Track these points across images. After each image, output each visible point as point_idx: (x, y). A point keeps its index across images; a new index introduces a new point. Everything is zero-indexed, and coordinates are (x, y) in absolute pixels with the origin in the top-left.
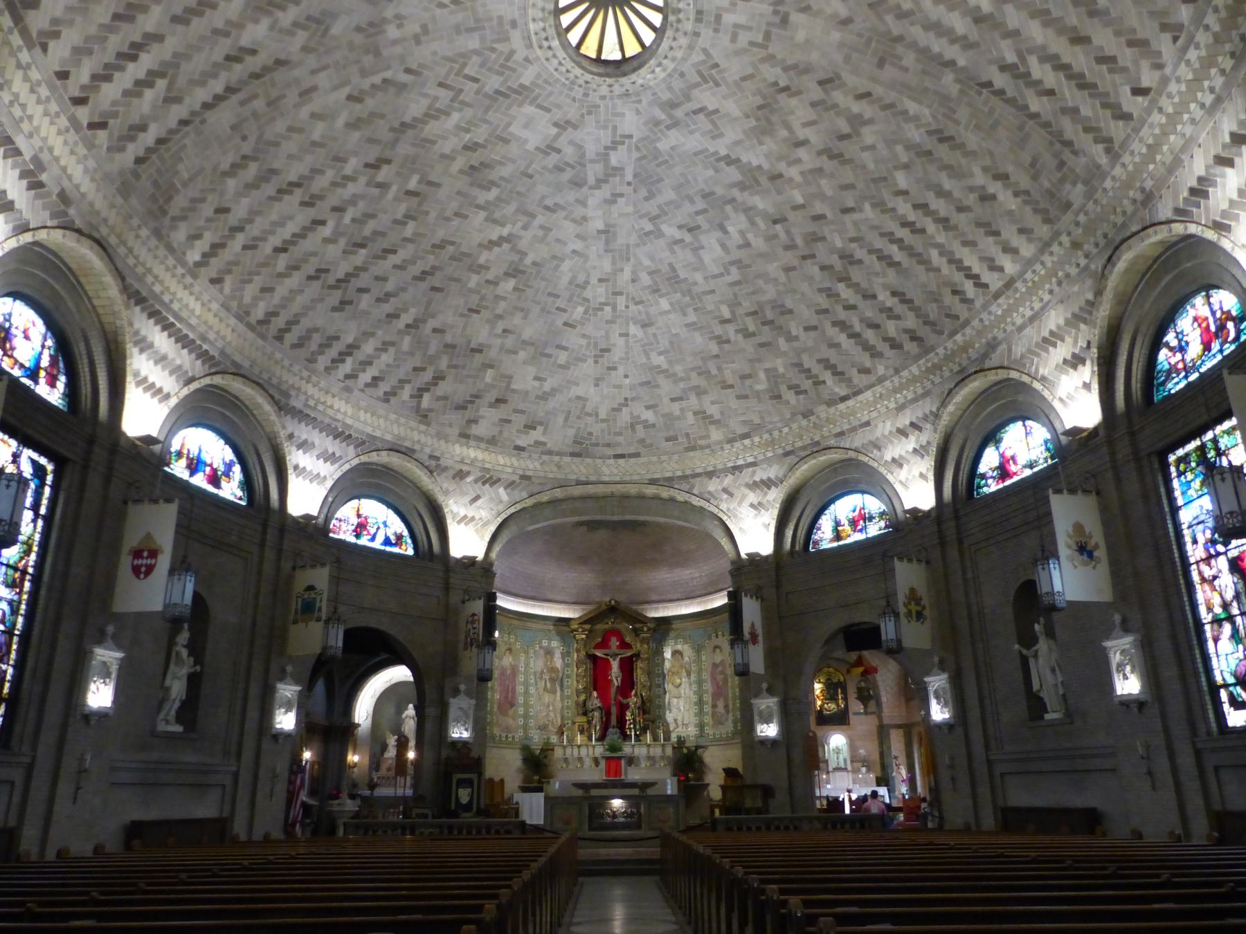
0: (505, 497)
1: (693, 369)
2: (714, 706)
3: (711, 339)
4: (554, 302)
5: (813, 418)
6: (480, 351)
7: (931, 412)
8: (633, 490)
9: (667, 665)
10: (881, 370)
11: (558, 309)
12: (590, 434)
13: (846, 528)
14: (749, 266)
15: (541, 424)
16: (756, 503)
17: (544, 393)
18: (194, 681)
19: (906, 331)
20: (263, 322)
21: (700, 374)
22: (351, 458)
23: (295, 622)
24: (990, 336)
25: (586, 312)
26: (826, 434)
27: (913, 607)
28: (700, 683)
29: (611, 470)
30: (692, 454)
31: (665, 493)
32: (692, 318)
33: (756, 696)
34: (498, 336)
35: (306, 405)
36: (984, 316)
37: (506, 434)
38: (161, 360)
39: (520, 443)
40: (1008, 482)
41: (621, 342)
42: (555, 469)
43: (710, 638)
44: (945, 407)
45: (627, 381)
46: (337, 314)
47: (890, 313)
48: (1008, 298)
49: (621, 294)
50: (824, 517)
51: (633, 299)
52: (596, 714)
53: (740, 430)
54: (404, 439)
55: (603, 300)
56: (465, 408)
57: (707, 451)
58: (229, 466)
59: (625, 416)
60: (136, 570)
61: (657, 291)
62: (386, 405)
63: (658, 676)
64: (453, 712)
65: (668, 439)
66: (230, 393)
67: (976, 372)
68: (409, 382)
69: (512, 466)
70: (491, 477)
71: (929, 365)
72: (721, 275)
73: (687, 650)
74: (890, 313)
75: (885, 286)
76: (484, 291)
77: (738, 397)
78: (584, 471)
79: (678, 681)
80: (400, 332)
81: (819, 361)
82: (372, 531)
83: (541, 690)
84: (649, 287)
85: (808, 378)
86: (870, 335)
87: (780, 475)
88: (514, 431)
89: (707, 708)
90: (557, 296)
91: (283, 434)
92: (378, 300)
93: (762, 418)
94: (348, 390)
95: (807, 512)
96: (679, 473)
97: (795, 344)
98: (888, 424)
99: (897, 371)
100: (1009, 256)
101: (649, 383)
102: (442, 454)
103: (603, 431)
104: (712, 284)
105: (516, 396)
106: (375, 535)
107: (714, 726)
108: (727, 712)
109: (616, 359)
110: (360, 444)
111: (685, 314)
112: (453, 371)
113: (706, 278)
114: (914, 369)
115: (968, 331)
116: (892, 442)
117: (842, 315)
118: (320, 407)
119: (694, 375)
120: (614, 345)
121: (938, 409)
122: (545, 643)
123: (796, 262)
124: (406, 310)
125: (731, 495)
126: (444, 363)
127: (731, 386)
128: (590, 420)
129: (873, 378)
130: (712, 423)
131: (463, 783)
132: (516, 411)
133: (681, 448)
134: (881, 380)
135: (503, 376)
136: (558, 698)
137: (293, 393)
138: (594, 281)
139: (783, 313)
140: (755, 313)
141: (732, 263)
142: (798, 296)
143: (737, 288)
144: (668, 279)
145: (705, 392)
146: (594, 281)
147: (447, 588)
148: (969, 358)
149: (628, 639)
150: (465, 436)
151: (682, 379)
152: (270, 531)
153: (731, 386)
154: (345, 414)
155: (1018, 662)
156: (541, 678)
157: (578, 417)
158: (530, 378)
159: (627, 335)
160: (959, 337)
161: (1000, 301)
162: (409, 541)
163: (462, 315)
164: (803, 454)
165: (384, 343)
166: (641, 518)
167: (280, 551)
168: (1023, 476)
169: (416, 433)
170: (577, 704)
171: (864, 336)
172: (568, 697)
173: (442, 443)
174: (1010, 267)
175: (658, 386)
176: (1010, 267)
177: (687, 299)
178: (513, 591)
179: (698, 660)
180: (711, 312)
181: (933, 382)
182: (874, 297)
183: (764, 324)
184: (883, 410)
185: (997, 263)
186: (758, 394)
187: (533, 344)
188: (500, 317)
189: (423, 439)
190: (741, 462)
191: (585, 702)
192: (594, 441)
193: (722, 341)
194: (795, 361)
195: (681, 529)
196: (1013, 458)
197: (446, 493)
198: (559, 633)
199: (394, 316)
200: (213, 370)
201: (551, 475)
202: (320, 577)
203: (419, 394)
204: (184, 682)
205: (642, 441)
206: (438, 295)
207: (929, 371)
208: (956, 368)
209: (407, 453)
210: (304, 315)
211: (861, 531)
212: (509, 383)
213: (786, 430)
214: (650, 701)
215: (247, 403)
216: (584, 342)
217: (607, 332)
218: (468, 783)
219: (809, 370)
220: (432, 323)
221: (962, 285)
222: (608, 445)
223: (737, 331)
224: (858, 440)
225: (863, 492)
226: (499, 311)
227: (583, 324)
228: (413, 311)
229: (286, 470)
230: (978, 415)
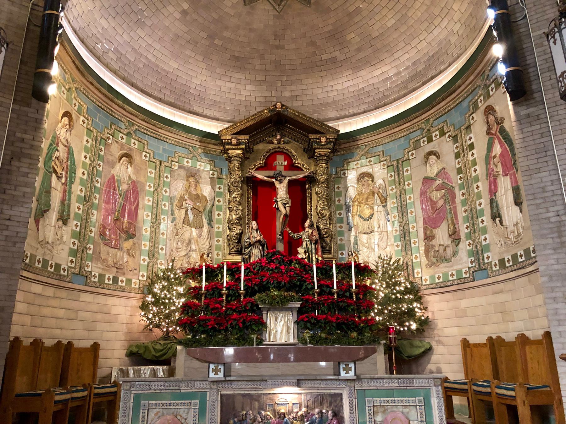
2: (428, 238)
9: (352, 192)
28: (403, 210)
43: (417, 146)
63: (340, 207)
79: (367, 212)
83: (180, 225)
107: (430, 265)
122: (187, 163)
149: (299, 162)
156: (180, 207)
172: (219, 234)
178: (139, 84)
191: (240, 235)
198: (207, 153)
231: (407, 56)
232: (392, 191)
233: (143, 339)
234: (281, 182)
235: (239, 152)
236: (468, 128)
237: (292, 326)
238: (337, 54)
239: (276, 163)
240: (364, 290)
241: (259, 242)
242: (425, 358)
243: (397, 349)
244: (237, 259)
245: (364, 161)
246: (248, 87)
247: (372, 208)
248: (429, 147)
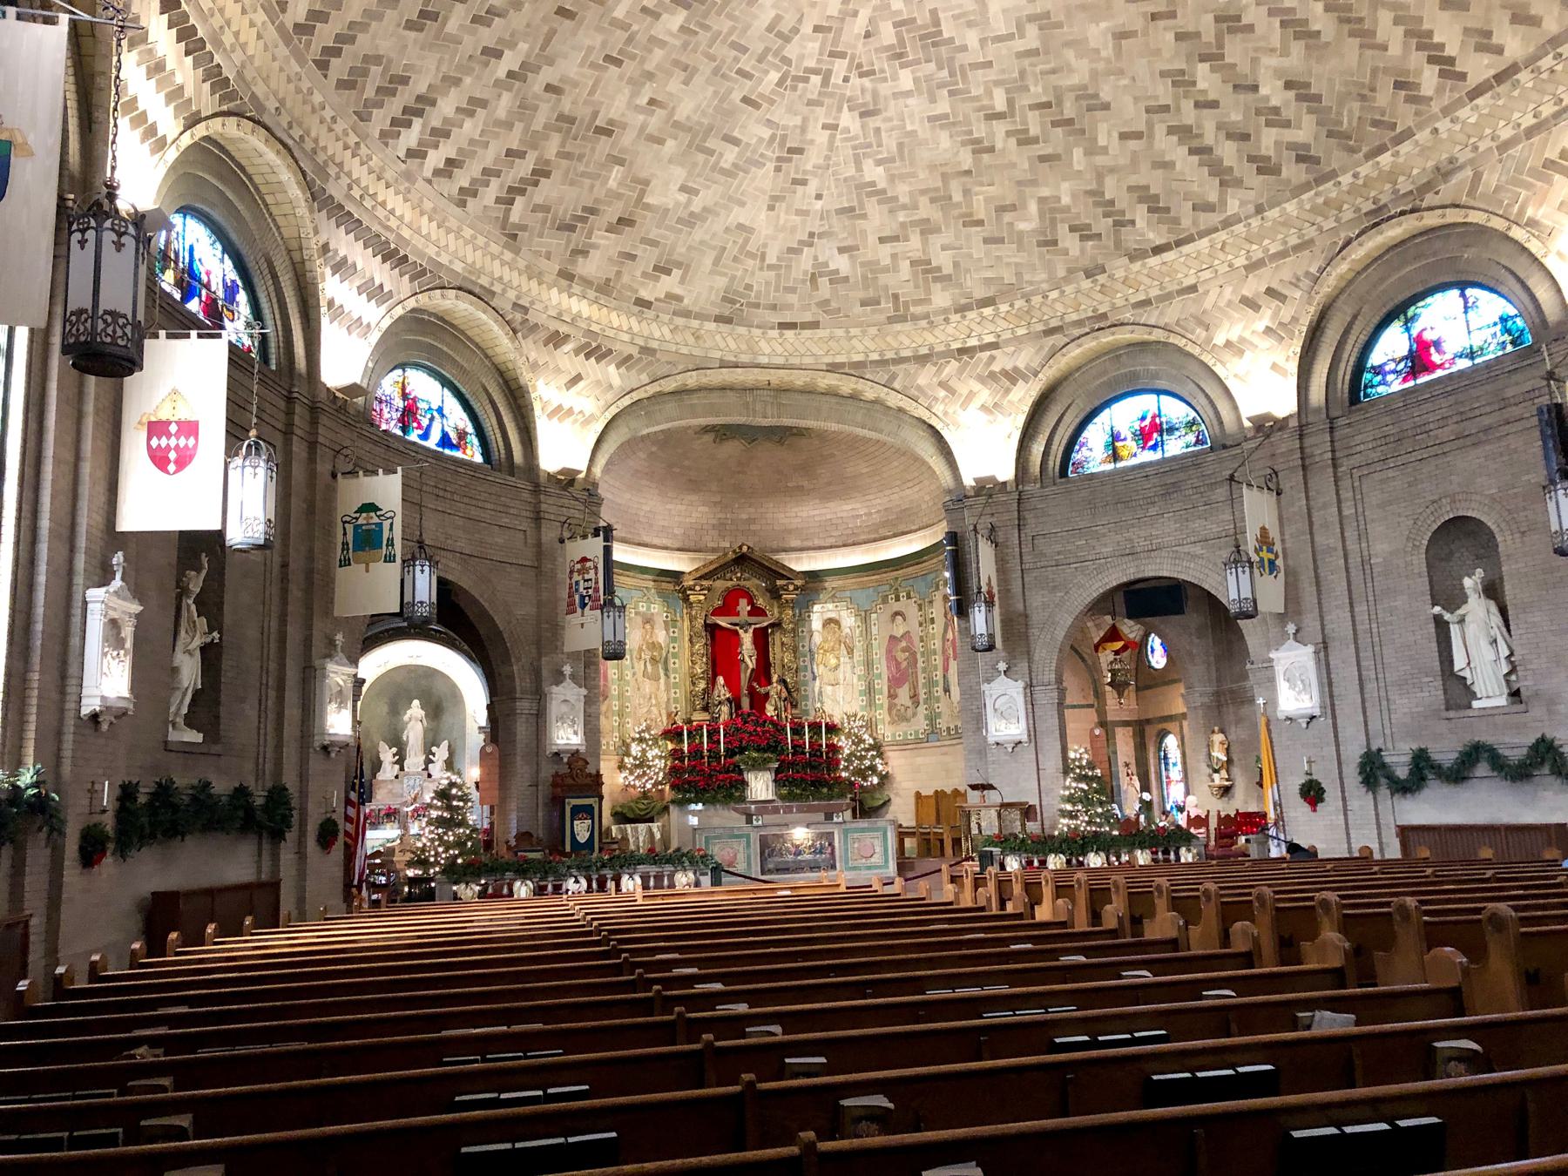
0: (616, 381)
1: (923, 192)
2: (892, 696)
3: (964, 144)
4: (736, 60)
5: (1101, 278)
6: (609, 133)
7: (1307, 274)
8: (799, 379)
10: (1233, 206)
11: (740, 72)
12: (749, 287)
13: (1129, 445)
14: (1059, 25)
15: (679, 265)
16: (990, 404)
17: (692, 214)
18: (210, 655)
19: (1292, 146)
20: (301, 29)
21: (933, 200)
22: (405, 296)
23: (345, 563)
24: (1445, 156)
25: (780, 83)
26: (1120, 303)
27: (1266, 555)
28: (869, 664)
29: (772, 347)
30: (898, 327)
31: (847, 385)
32: (943, 106)
33: (989, 681)
34: (638, 109)
35: (349, 197)
36: (1443, 125)
37: (625, 279)
38: (157, 68)
39: (645, 294)
40: (1424, 379)
41: (822, 137)
42: (691, 340)
43: (885, 600)
44: (1334, 268)
45: (819, 205)
46: (412, 34)
47: (1274, 117)
48: (1499, 96)
49: (842, 55)
50: (1090, 427)
51: (860, 66)
52: (725, 709)
53: (980, 293)
54: (480, 272)
55: (812, 64)
56: (572, 228)
57: (924, 323)
58: (231, 291)
59: (805, 262)
60: (159, 460)
61: (900, 56)
62: (458, 210)
64: (555, 708)
65: (864, 303)
66: (232, 159)
67: (1403, 213)
68: (498, 174)
69: (630, 331)
70: (598, 347)
71: (1320, 200)
72: (1010, 37)
73: (849, 621)
74: (1274, 117)
75: (1278, 72)
76: (635, 27)
77: (986, 241)
78: (733, 346)
79: (833, 662)
80: (497, 83)
81: (1130, 189)
82: (425, 422)
84: (891, 47)
85: (1106, 215)
86: (1228, 152)
87: (1035, 365)
88: (638, 273)
89: (882, 699)
90: (744, 50)
91: (313, 244)
92: (476, 20)
93: (1019, 275)
94: (409, 176)
95: (1068, 419)
96: (875, 357)
97: (1100, 160)
98: (1228, 290)
99: (1259, 210)
100: (1522, 28)
101: (852, 209)
102: (532, 303)
103: (768, 283)
104: (992, 50)
105: (649, 214)
106: (429, 427)
107: (892, 722)
108: (917, 704)
109: (809, 167)
110: (418, 274)
111: (933, 100)
112: (564, 163)
113: (983, 42)
114: (1291, 207)
115: (1405, 148)
116: (1229, 318)
117: (1188, 114)
118: (368, 203)
119: (924, 201)
120: (812, 142)
121: (1322, 270)
122: (642, 608)
123: (1138, 25)
124: (512, 45)
125: (952, 392)
126: (552, 147)
127: (980, 223)
128: (750, 263)
129: (1214, 218)
130: (936, 280)
131: (578, 812)
132: (645, 241)
133: (883, 318)
134: (1227, 224)
135: (636, 180)
136: (662, 686)
137: (332, 171)
138: (807, 28)
139: (1090, 109)
140: (1048, 105)
141: (1032, 18)
142: (1125, 82)
143: (1026, 62)
144: (922, 38)
145: (937, 230)
146: (807, 28)
147: (537, 518)
148: (1395, 192)
149: (760, 602)
150: (567, 275)
151: (904, 207)
152: (298, 409)
153: (980, 223)
154: (401, 218)
155: (1432, 628)
157: (735, 259)
158: (674, 187)
159: (835, 127)
160: (1385, 159)
161: (1479, 101)
162: (476, 441)
163: (593, 66)
164: (1076, 332)
165: (472, 100)
166: (803, 423)
167: (312, 445)
168: (1454, 369)
169: (497, 263)
170: (693, 694)
171: (1218, 152)
173: (534, 283)
174: (1515, 44)
175: (864, 216)
176: (1515, 44)
177: (945, 73)
179: (867, 631)
180: (977, 99)
181: (1320, 229)
182: (1255, 88)
183: (1055, 124)
184: (1225, 268)
185: (1495, 40)
186: (1019, 238)
187: (690, 129)
188: (650, 76)
189: (507, 274)
190: (973, 342)
192: (753, 300)
193: (981, 148)
194: (1093, 186)
195: (854, 443)
196: (1437, 344)
197: (534, 367)
198: (661, 594)
199: (494, 53)
200: (225, 108)
201: (685, 350)
202: (387, 489)
203: (507, 202)
204: (198, 653)
205: (824, 304)
206: (567, 22)
207: (1314, 210)
208: (1368, 206)
209: (482, 296)
210: (364, 27)
211: (1154, 448)
212: (642, 193)
213: (1054, 295)
214: (797, 690)
215: (257, 179)
216: (766, 133)
217: (805, 120)
218: (587, 812)
219: (1112, 203)
220: (547, 75)
221: (1419, 72)
222: (774, 307)
223: (1009, 134)
224: (1171, 313)
225: (1159, 392)
226: (649, 66)
227: (772, 102)
228: (523, 46)
229: (318, 306)
230: (1382, 280)
231: (878, 501)
232: (859, 646)
233: (621, 800)
234: (746, 631)
235: (702, 598)
236: (931, 602)
237: (770, 784)
238: (805, 483)
239: (739, 608)
240: (833, 749)
241: (728, 699)
242: (884, 809)
243: (861, 803)
244: (699, 717)
245: (830, 606)
246: (700, 509)
247: (838, 658)
248: (896, 607)
